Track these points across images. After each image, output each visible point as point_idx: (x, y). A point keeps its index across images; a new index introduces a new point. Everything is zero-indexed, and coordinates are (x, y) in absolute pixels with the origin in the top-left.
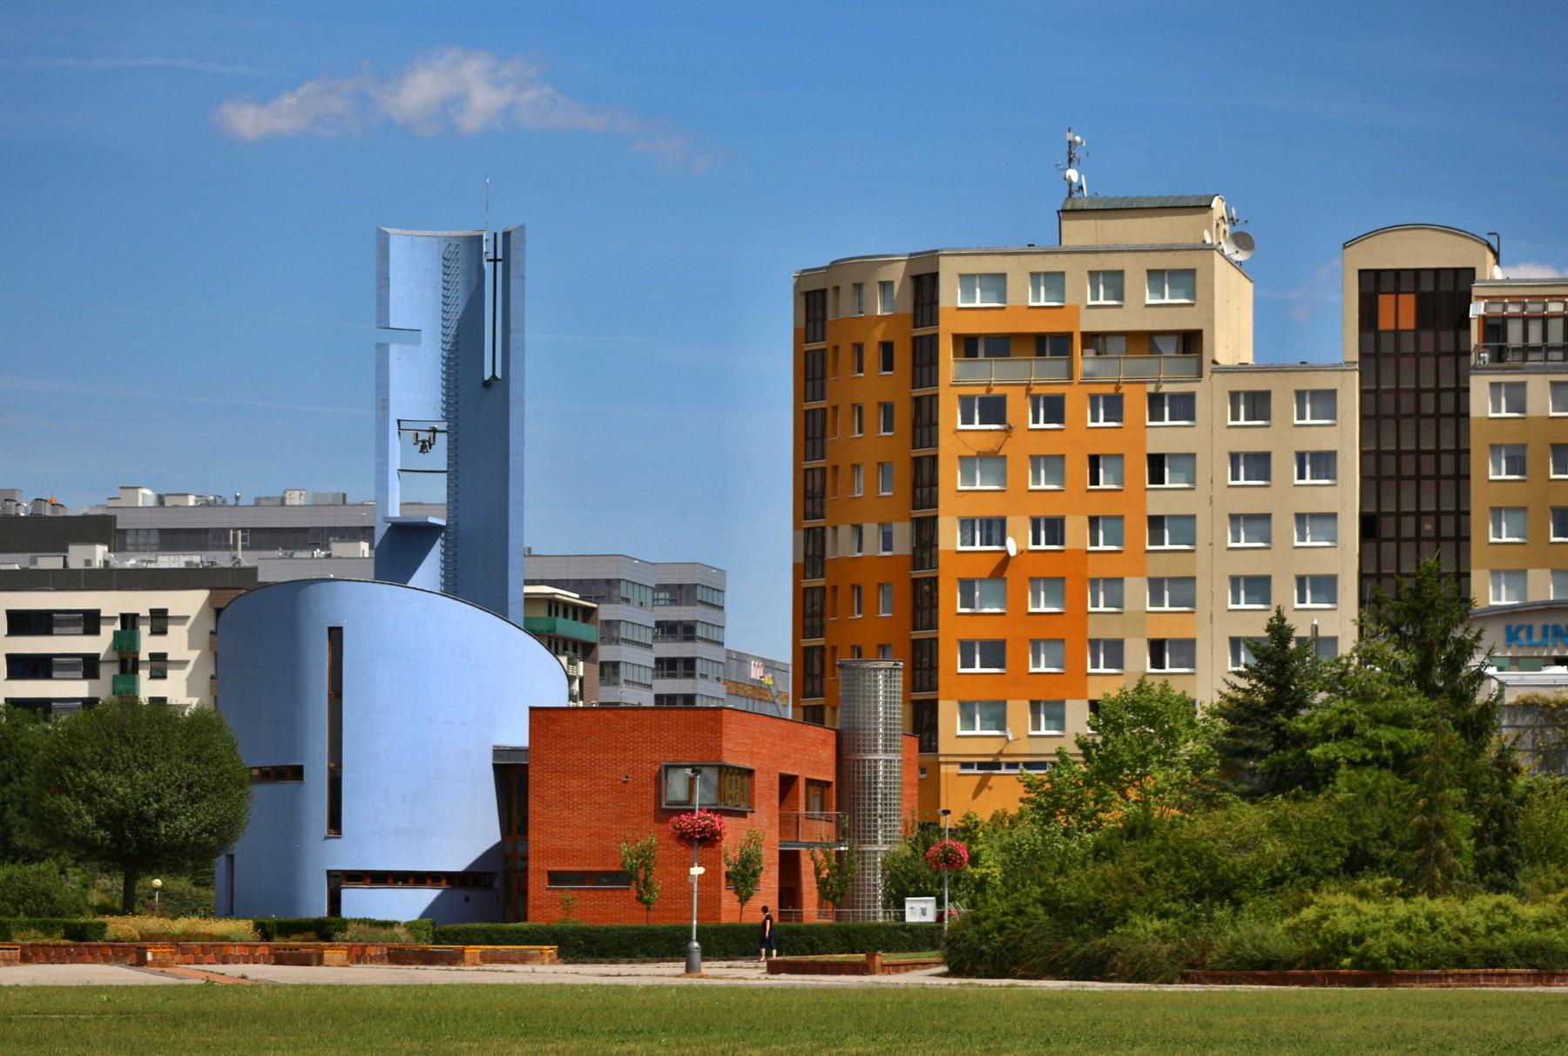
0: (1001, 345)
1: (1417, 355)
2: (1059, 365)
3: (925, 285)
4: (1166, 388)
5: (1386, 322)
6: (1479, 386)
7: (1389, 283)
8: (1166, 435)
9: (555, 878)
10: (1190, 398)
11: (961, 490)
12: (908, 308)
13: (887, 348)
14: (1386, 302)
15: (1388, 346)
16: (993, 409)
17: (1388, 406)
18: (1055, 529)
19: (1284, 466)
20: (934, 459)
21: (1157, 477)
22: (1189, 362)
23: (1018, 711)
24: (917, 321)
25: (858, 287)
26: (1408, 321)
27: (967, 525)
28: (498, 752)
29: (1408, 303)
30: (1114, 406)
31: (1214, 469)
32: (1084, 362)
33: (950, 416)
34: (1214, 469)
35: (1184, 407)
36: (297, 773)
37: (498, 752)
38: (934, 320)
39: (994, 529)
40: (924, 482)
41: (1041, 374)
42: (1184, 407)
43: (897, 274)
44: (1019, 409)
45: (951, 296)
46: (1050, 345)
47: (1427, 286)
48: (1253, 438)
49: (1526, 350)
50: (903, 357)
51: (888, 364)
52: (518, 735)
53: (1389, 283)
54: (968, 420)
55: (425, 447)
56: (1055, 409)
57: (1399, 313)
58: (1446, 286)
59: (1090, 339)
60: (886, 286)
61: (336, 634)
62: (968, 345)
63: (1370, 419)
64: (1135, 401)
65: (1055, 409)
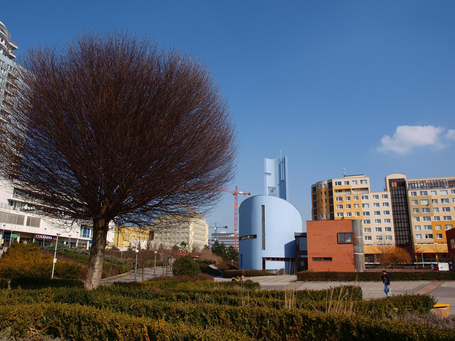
0: (340, 191)
1: (398, 190)
2: (349, 192)
3: (330, 184)
4: (364, 195)
5: (393, 186)
6: (409, 193)
7: (392, 181)
8: (364, 201)
9: (315, 259)
10: (367, 196)
11: (337, 209)
12: (327, 187)
13: (325, 192)
14: (392, 183)
15: (393, 189)
16: (341, 199)
17: (394, 197)
18: (350, 214)
19: (381, 205)
20: (333, 206)
21: (364, 206)
22: (367, 192)
23: (421, 218)
24: (329, 188)
25: (321, 185)
26: (396, 186)
27: (338, 214)
28: (295, 233)
29: (396, 183)
30: (357, 198)
31: (371, 205)
32: (353, 192)
33: (335, 199)
34: (371, 205)
35: (367, 197)
36: (255, 236)
37: (295, 233)
38: (332, 188)
39: (342, 214)
40: (332, 209)
41: (347, 194)
42: (367, 197)
43: (326, 182)
44: (344, 198)
45: (334, 184)
46: (349, 190)
47: (398, 181)
48: (376, 201)
49: (415, 188)
50: (327, 193)
51: (325, 194)
52: (300, 230)
53: (392, 181)
54: (337, 200)
55: (272, 191)
56: (349, 198)
57: (395, 185)
58: (401, 181)
59: (353, 189)
60: (325, 184)
61: (263, 206)
62: (336, 191)
63: (392, 198)
64: (360, 198)
65: (349, 198)
